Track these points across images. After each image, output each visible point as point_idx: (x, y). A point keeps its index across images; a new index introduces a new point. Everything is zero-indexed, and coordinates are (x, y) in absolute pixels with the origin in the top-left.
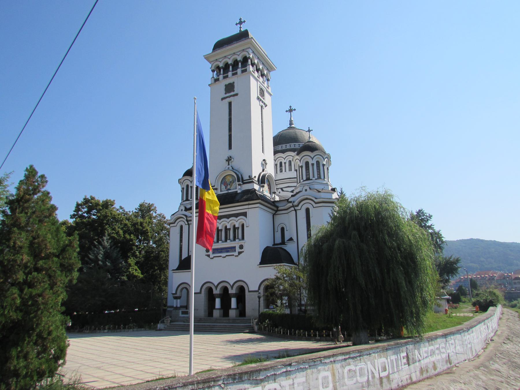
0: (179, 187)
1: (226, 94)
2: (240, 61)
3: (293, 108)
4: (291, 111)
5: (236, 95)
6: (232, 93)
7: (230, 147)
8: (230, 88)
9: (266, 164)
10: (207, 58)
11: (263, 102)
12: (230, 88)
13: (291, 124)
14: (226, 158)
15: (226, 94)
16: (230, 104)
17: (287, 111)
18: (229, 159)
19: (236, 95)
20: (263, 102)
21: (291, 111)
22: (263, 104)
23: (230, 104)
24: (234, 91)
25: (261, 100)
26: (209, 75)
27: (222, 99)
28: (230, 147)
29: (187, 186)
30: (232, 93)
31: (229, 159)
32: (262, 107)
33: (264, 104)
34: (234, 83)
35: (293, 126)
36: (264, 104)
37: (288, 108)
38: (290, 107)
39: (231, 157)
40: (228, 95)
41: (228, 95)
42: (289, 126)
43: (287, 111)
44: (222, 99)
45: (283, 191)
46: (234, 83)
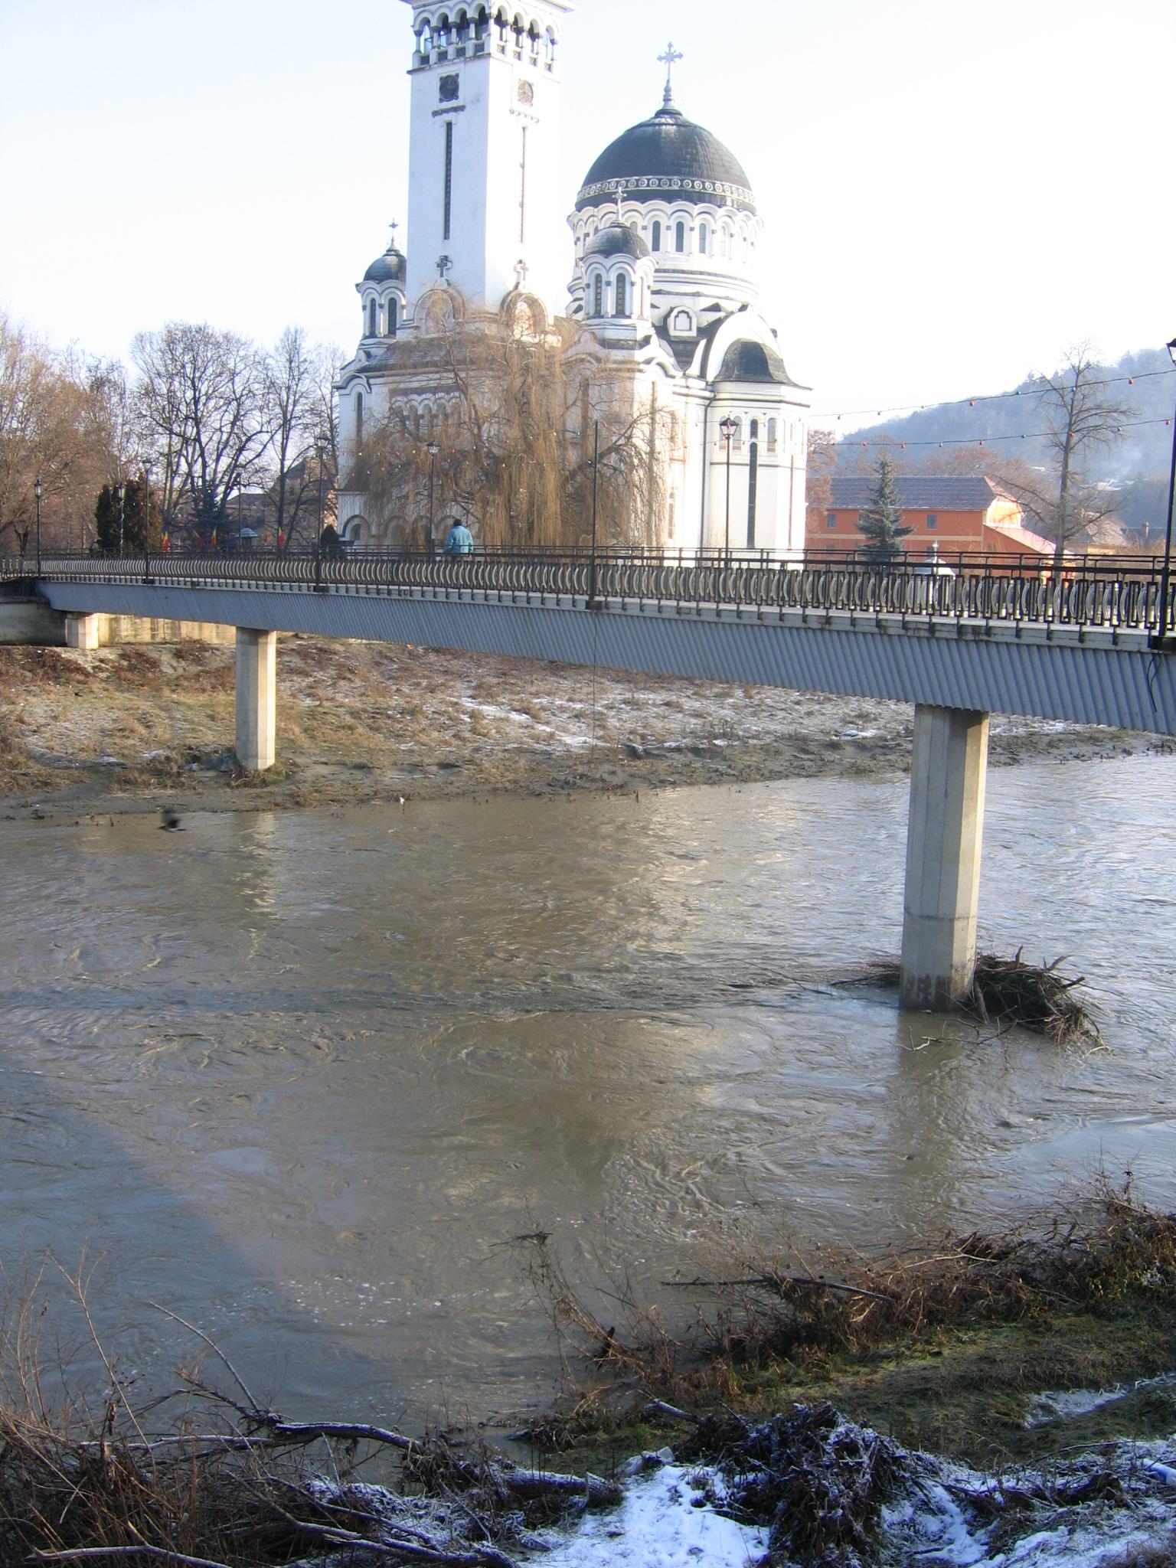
0: (357, 301)
1: (441, 101)
2: (473, 20)
3: (677, 49)
4: (670, 57)
5: (462, 108)
7: (446, 235)
8: (449, 88)
9: (525, 269)
12: (449, 88)
13: (667, 99)
14: (438, 260)
15: (441, 101)
16: (449, 125)
17: (660, 59)
18: (444, 262)
19: (462, 108)
21: (670, 57)
22: (527, 122)
23: (449, 125)
24: (457, 98)
26: (405, 45)
27: (435, 114)
28: (446, 235)
29: (373, 300)
31: (444, 262)
34: (457, 75)
35: (675, 105)
38: (670, 46)
39: (446, 258)
42: (660, 106)
43: (660, 59)
44: (435, 114)
46: (457, 75)
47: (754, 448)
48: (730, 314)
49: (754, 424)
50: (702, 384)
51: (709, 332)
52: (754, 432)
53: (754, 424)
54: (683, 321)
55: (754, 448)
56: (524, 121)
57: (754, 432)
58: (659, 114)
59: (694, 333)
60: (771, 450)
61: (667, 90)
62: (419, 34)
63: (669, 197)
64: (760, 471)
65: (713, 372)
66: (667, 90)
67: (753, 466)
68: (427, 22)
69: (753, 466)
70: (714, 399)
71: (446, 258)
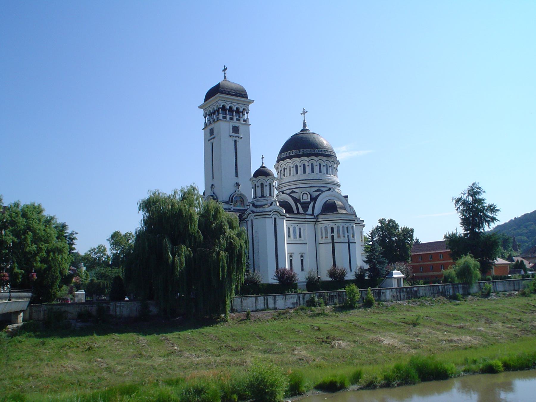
4: (304, 113)
6: (213, 136)
8: (212, 132)
10: (200, 107)
11: (236, 137)
12: (212, 132)
13: (305, 125)
20: (236, 137)
21: (304, 113)
25: (233, 136)
27: (209, 140)
30: (213, 136)
32: (236, 141)
33: (239, 137)
35: (307, 128)
36: (239, 137)
37: (302, 111)
40: (211, 137)
41: (211, 137)
45: (283, 193)
47: (333, 237)
48: (323, 192)
49: (332, 229)
50: (313, 217)
51: (314, 199)
52: (332, 231)
53: (332, 229)
54: (305, 196)
55: (333, 237)
56: (235, 139)
57: (332, 231)
58: (302, 131)
59: (309, 200)
60: (339, 237)
61: (304, 123)
62: (205, 117)
63: (308, 156)
64: (335, 244)
65: (317, 212)
66: (304, 123)
67: (333, 243)
68: (206, 113)
69: (333, 243)
70: (317, 221)
71: (213, 185)
